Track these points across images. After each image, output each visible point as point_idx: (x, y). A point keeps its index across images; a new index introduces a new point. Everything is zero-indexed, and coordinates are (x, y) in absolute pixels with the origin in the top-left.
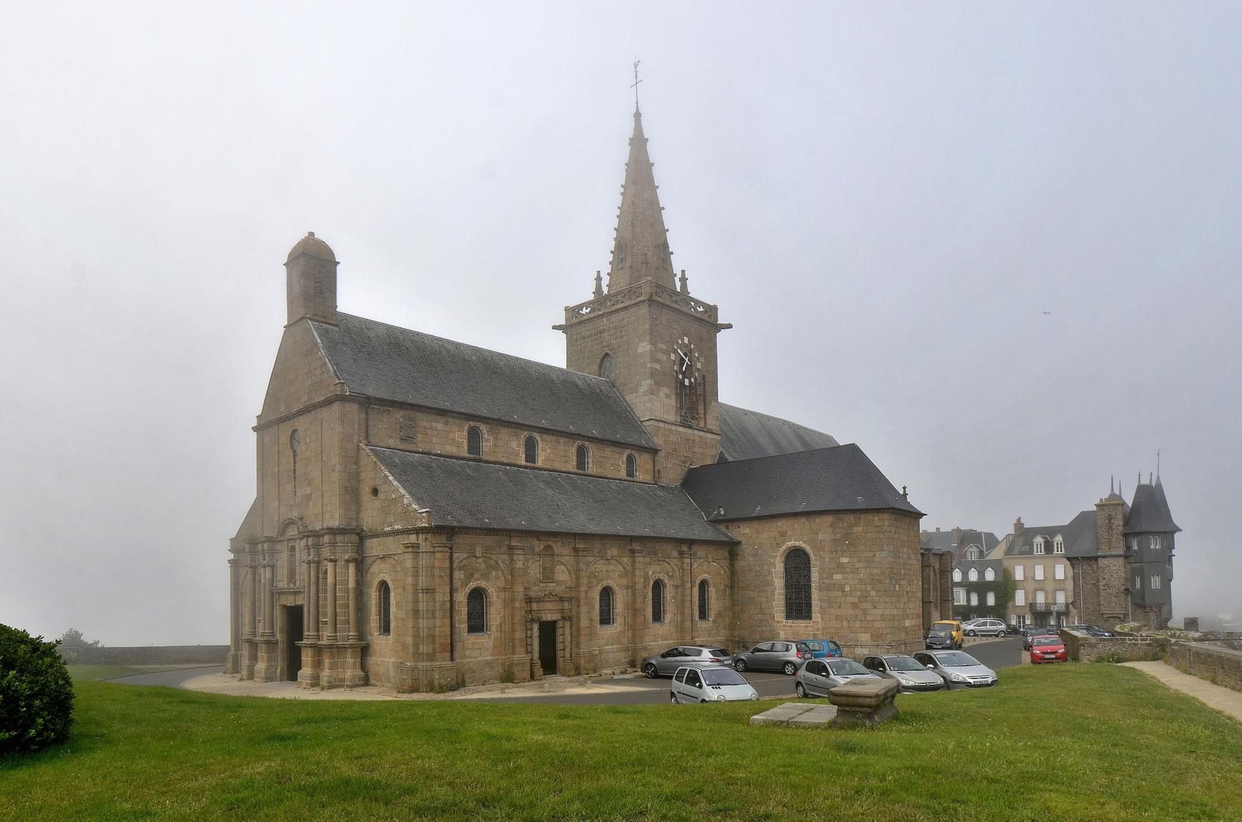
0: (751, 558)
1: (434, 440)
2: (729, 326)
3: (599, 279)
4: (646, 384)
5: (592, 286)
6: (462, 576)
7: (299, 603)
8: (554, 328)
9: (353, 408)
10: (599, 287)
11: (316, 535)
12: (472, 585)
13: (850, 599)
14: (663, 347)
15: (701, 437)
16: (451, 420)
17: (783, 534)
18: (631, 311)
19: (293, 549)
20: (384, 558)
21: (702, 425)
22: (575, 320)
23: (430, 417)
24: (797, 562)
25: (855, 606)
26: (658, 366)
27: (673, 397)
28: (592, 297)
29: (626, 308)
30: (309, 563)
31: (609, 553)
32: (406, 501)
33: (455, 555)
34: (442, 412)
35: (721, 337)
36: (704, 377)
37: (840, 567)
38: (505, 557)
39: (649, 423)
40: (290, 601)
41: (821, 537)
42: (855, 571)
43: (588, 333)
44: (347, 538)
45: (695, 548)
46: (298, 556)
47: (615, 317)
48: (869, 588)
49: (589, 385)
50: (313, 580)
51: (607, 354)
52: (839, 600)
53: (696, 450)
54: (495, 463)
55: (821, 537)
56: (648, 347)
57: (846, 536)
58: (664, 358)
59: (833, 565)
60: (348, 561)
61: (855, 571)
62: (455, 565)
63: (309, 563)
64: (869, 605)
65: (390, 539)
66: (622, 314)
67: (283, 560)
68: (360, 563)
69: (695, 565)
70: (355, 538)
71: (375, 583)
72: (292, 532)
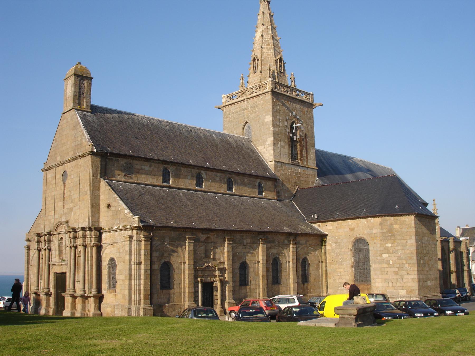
0: (334, 245)
6: (157, 255)
7: (64, 271)
11: (74, 230)
12: (163, 261)
13: (393, 269)
14: (281, 118)
17: (352, 230)
21: (305, 163)
24: (360, 247)
25: (396, 273)
26: (277, 130)
27: (287, 147)
29: (258, 96)
31: (245, 241)
33: (154, 243)
34: (148, 160)
35: (316, 111)
36: (306, 135)
37: (387, 250)
42: (395, 252)
43: (235, 110)
45: (299, 238)
46: (64, 244)
47: (251, 101)
48: (404, 262)
49: (236, 141)
50: (73, 257)
52: (387, 270)
53: (301, 179)
54: (179, 188)
55: (374, 231)
58: (281, 125)
61: (395, 252)
62: (154, 248)
63: (71, 247)
64: (404, 273)
65: (117, 233)
67: (55, 245)
69: (299, 249)
71: (108, 260)
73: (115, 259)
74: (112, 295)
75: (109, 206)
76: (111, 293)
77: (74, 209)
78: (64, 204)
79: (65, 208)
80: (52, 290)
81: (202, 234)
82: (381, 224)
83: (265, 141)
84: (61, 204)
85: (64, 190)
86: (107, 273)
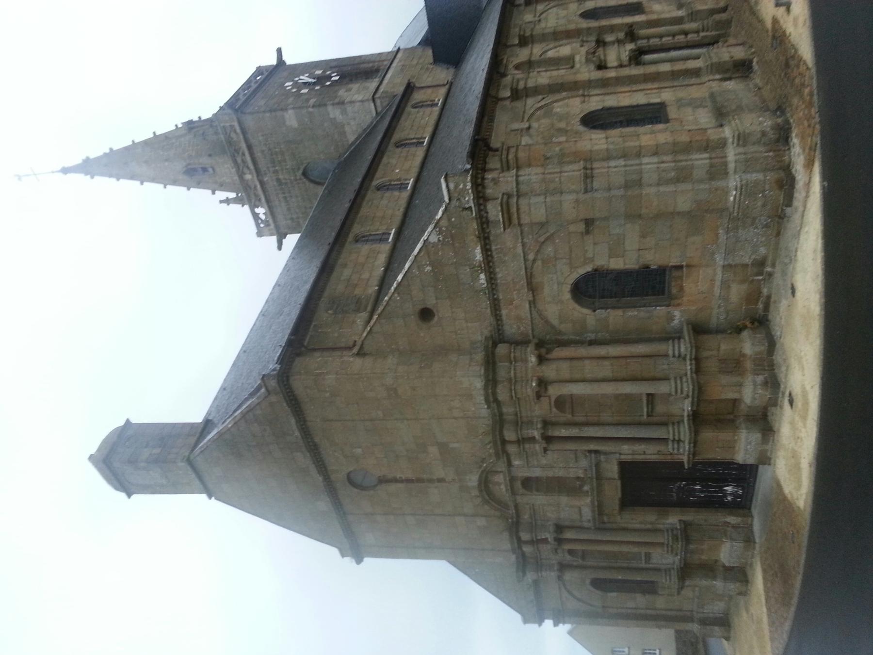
1: (366, 276)
2: (279, 51)
3: (227, 201)
4: (334, 113)
5: (236, 207)
7: (615, 468)
10: (236, 201)
15: (400, 61)
16: (340, 261)
18: (253, 141)
19: (528, 483)
20: (532, 287)
28: (247, 207)
29: (250, 147)
30: (548, 439)
32: (434, 239)
38: (530, 101)
39: (378, 102)
40: (613, 492)
51: (305, 174)
56: (290, 112)
65: (501, 274)
66: (258, 155)
68: (546, 345)
70: (502, 349)
72: (501, 488)
73: (575, 276)
74: (689, 286)
75: (426, 314)
76: (681, 289)
78: (430, 481)
80: (673, 519)
81: (504, 75)
83: (333, 121)
85: (396, 480)
86: (619, 312)
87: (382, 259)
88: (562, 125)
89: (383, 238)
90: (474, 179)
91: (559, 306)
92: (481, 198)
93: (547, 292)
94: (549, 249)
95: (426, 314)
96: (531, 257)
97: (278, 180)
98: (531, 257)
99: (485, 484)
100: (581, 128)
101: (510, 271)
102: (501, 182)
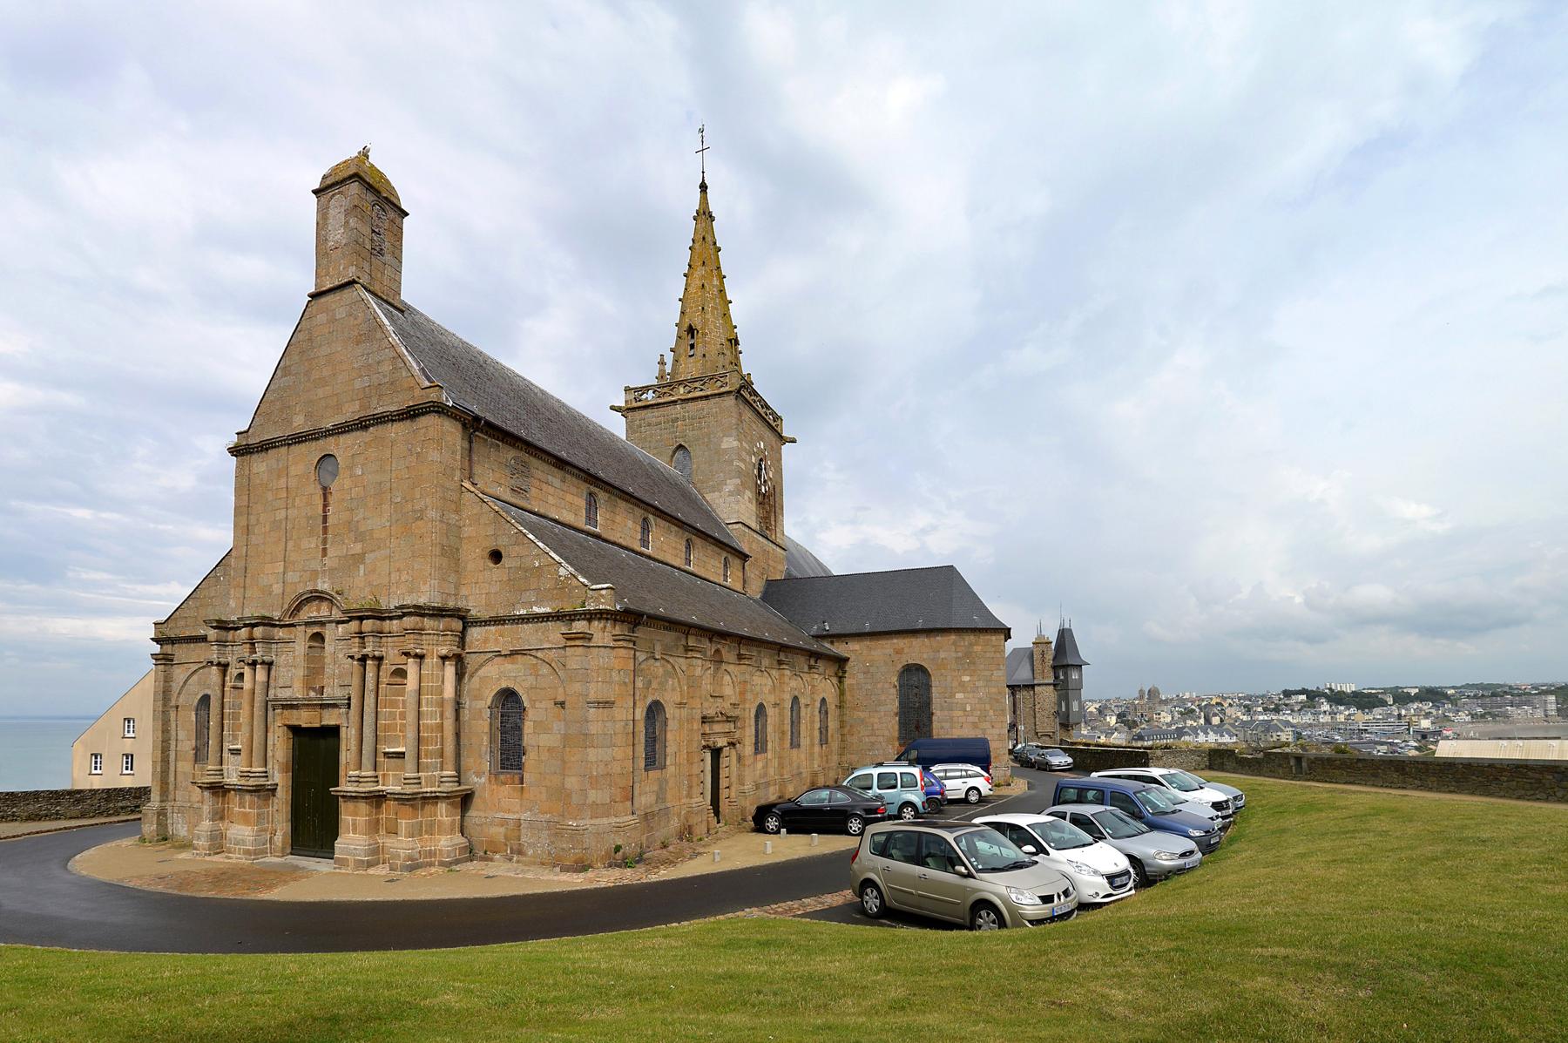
0: (861, 676)
1: (551, 499)
3: (662, 363)
8: (612, 408)
9: (451, 431)
10: (662, 371)
18: (713, 401)
22: (635, 405)
23: (546, 467)
29: (707, 397)
32: (562, 571)
41: (943, 655)
42: (975, 689)
44: (442, 624)
45: (820, 664)
55: (943, 655)
57: (967, 655)
59: (955, 684)
60: (444, 658)
66: (701, 404)
72: (311, 612)
75: (496, 556)
77: (369, 557)
78: (325, 541)
79: (330, 553)
82: (954, 643)
84: (313, 543)
87: (568, 517)
88: (654, 685)
89: (591, 519)
90: (607, 612)
91: (491, 677)
92: (590, 616)
93: (508, 666)
94: (545, 670)
95: (496, 556)
96: (539, 654)
97: (675, 420)
98: (539, 654)
99: (318, 597)
100: (649, 701)
101: (528, 635)
102: (602, 633)
